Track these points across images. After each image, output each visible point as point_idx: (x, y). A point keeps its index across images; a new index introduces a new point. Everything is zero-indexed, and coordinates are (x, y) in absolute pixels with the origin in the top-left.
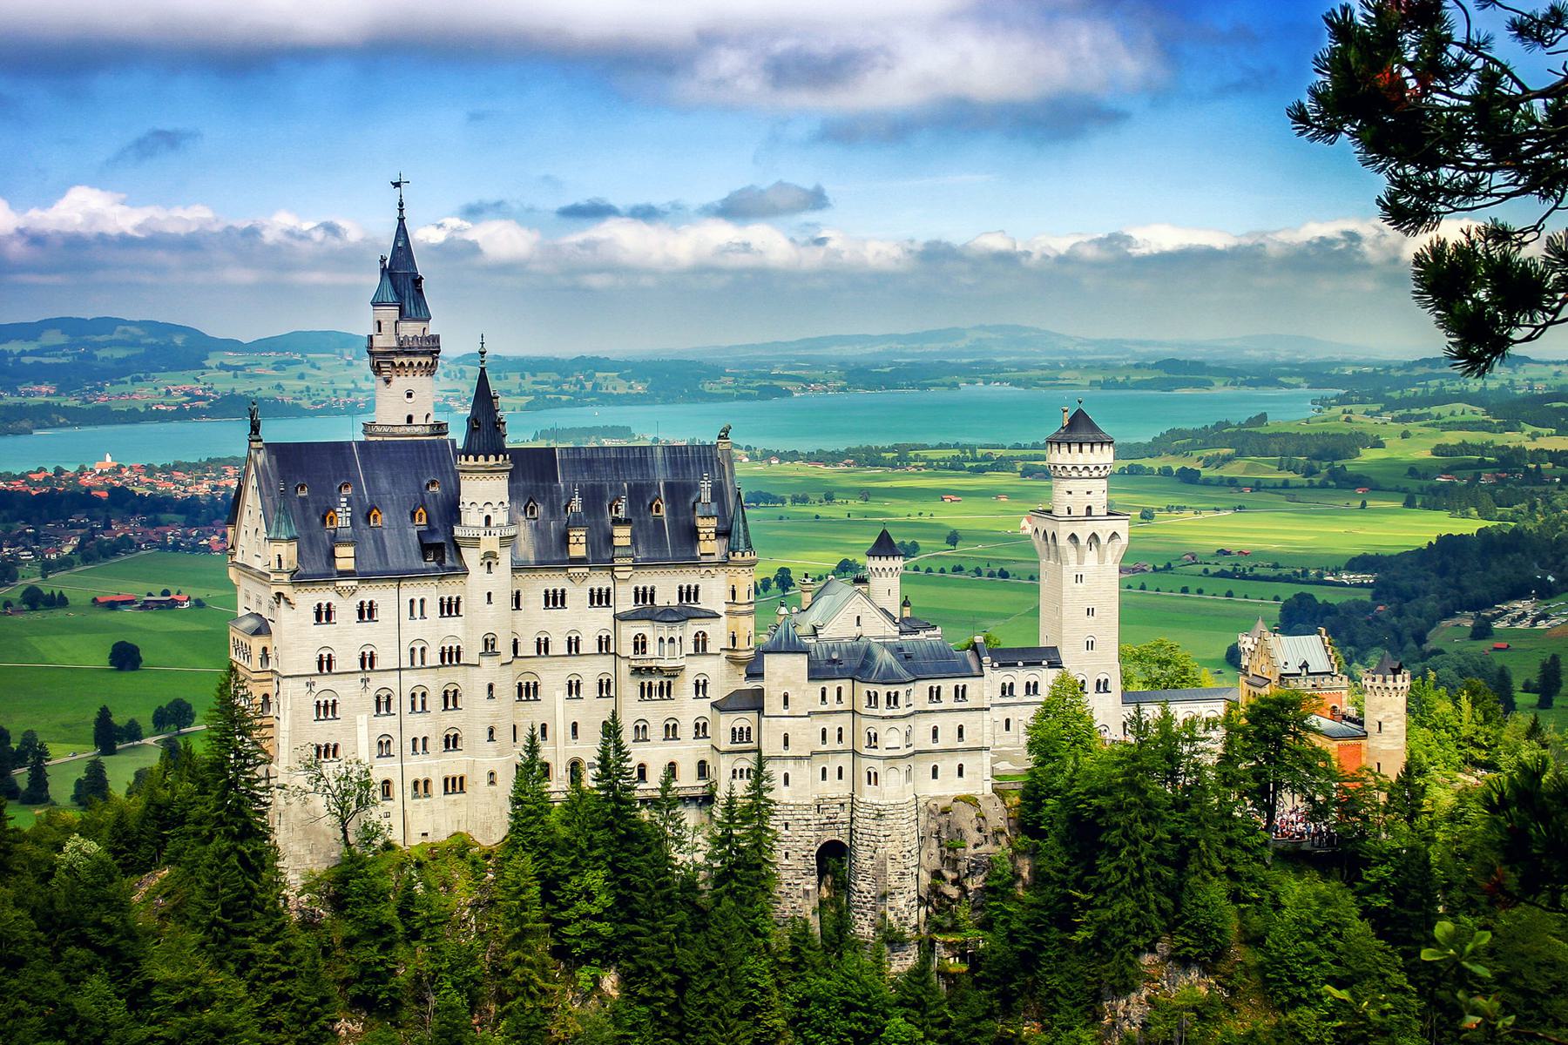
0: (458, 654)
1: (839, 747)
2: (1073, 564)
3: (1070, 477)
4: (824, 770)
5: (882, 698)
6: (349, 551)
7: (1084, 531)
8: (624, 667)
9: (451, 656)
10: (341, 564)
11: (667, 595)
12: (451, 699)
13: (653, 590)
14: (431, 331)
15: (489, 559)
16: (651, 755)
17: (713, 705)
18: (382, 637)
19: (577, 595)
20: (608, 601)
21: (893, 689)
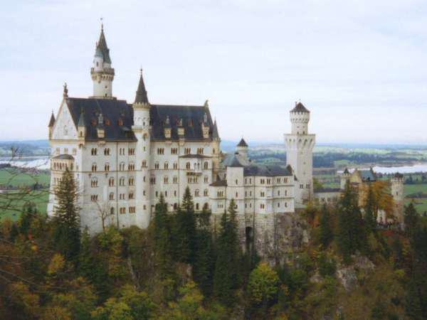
5: (266, 181)
6: (103, 132)
10: (100, 136)
11: (194, 152)
12: (131, 181)
15: (144, 137)
16: (195, 200)
17: (210, 185)
18: (111, 160)
19: (167, 151)
21: (269, 178)
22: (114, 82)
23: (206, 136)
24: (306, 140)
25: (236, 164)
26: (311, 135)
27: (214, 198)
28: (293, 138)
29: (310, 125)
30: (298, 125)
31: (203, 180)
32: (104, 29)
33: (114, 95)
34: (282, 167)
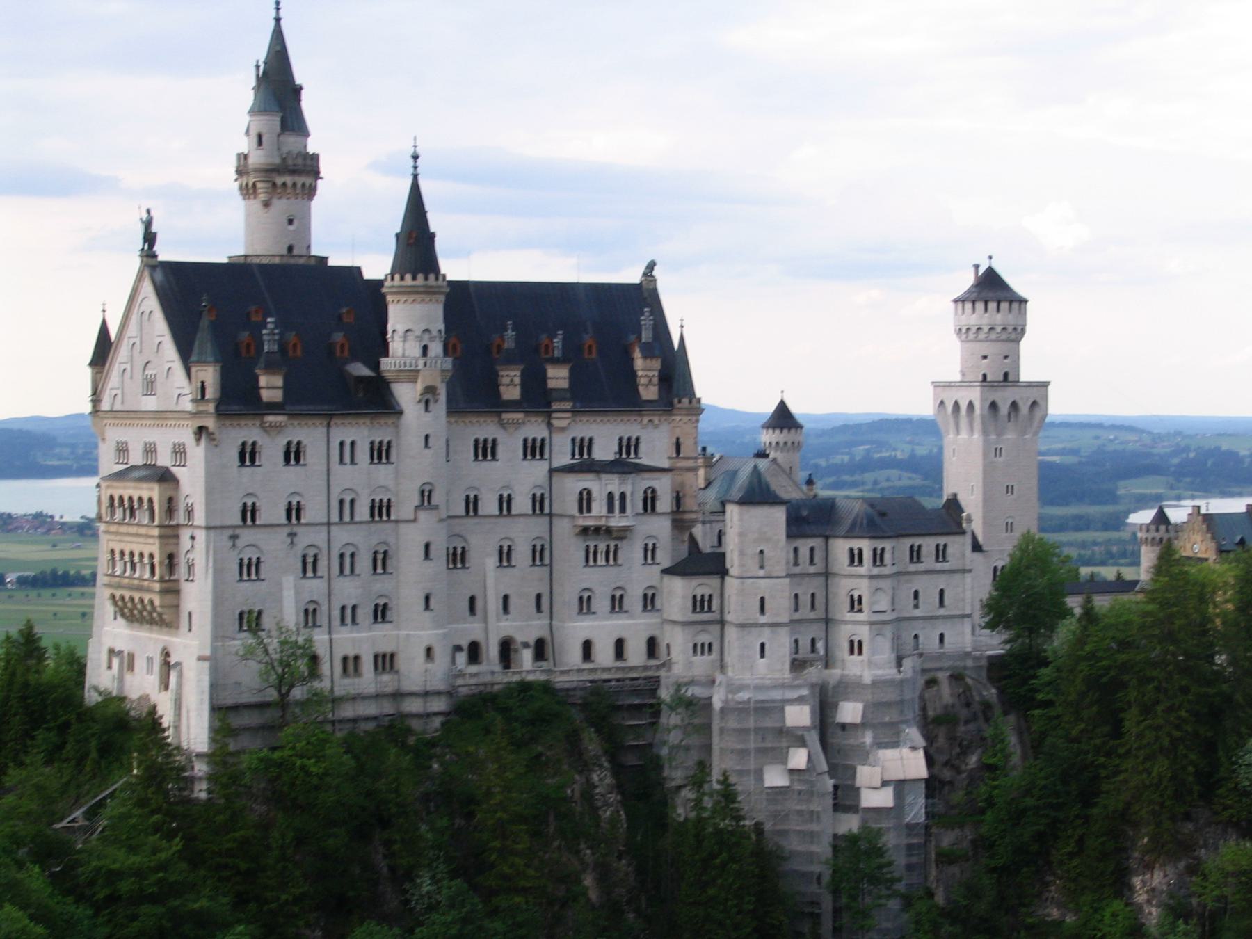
0: (389, 508)
1: (812, 615)
2: (993, 437)
3: (987, 340)
4: (796, 641)
5: (867, 555)
7: (1004, 398)
8: (564, 529)
9: (381, 510)
10: (266, 395)
11: (604, 451)
12: (381, 561)
13: (591, 440)
14: (311, 149)
17: (666, 571)
20: (542, 454)
21: (880, 544)
22: (317, 205)
23: (649, 392)
24: (1014, 405)
25: (758, 494)
26: (1030, 385)
27: (679, 618)
28: (964, 397)
29: (1027, 346)
30: (985, 348)
31: (641, 554)
32: (282, 13)
33: (316, 251)
34: (930, 503)
